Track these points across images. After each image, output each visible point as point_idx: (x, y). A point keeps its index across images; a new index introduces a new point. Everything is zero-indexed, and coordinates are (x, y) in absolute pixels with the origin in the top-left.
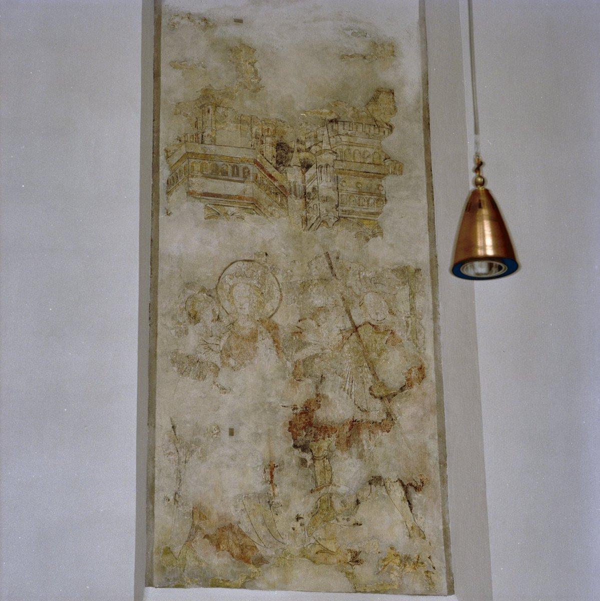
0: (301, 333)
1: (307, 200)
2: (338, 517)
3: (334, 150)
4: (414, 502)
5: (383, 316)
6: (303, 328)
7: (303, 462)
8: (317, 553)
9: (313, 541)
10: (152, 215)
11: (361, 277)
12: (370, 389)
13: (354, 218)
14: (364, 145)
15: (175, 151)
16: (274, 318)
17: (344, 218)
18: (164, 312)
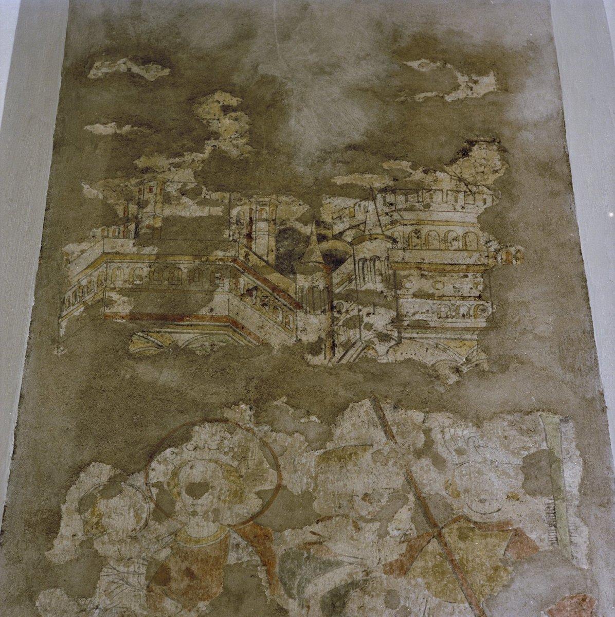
0: (320, 543)
1: (336, 314)
5: (496, 506)
6: (326, 534)
10: (27, 356)
11: (447, 436)
13: (428, 339)
15: (82, 252)
16: (263, 519)
17: (410, 339)
18: (35, 519)
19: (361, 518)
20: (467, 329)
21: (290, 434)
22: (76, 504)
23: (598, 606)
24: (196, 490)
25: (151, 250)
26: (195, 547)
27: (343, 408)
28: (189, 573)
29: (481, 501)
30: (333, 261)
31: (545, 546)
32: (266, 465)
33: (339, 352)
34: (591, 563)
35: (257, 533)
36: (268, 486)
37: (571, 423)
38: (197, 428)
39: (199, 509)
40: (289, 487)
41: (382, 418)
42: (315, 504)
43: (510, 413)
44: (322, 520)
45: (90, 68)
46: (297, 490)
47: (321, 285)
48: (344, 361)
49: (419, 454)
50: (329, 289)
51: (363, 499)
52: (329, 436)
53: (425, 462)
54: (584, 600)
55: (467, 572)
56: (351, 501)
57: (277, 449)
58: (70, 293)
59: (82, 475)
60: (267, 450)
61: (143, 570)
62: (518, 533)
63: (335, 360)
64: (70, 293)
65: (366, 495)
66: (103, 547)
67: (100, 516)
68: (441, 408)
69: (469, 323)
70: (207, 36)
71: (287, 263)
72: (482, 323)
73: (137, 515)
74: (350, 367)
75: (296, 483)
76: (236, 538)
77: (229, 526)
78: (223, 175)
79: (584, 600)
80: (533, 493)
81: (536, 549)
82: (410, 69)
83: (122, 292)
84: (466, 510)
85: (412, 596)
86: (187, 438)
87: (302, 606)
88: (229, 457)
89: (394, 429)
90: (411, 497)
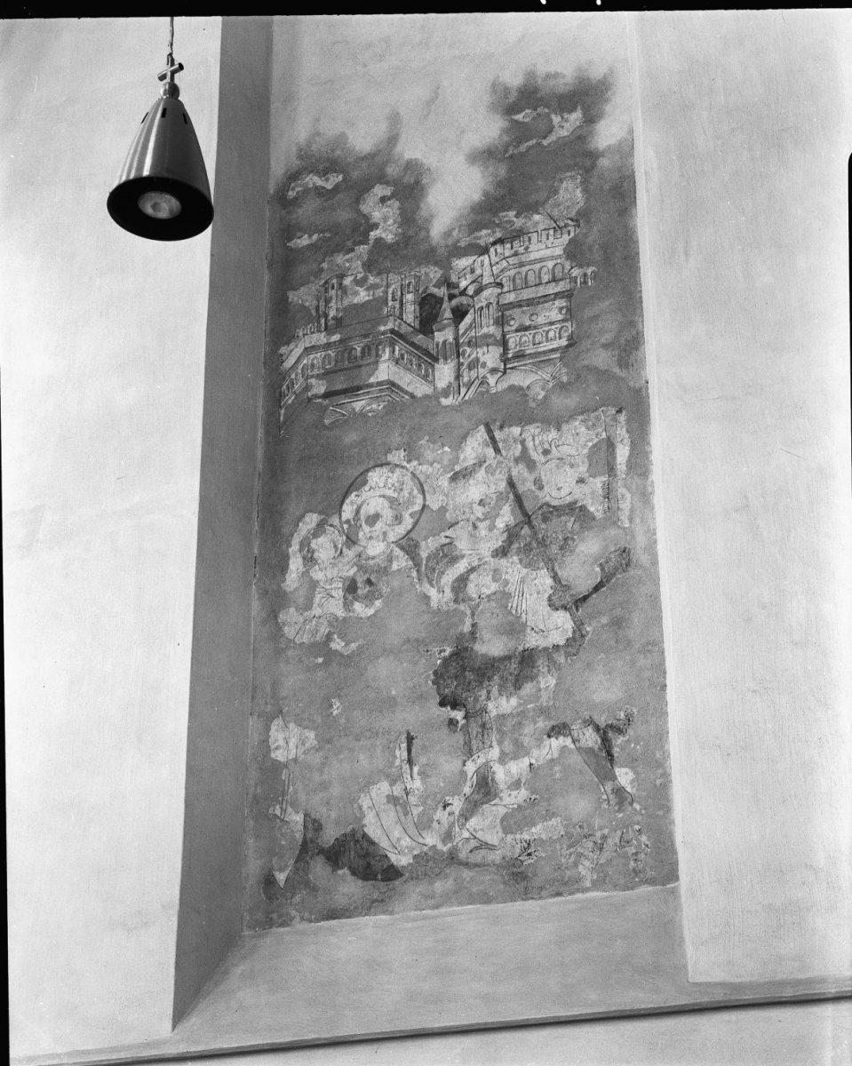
2: (501, 795)
3: (498, 280)
4: (616, 751)
7: (452, 723)
8: (471, 851)
9: (466, 835)
11: (537, 442)
12: (550, 599)
14: (541, 260)
15: (291, 351)
19: (478, 519)
20: (553, 350)
21: (431, 464)
22: (298, 547)
23: (633, 554)
24: (373, 519)
25: (336, 337)
26: (371, 562)
27: (464, 438)
28: (369, 582)
29: (558, 489)
30: (459, 314)
31: (599, 515)
32: (416, 492)
33: (463, 390)
34: (631, 522)
35: (409, 546)
36: (417, 508)
37: (624, 412)
38: (370, 474)
39: (374, 535)
40: (431, 505)
41: (493, 439)
42: (447, 515)
43: (582, 413)
44: (451, 526)
45: (288, 190)
46: (435, 507)
47: (451, 339)
48: (467, 398)
49: (517, 460)
50: (456, 339)
51: (479, 504)
52: (456, 460)
53: (521, 466)
54: (624, 551)
55: (546, 546)
56: (471, 508)
57: (422, 479)
58: (285, 387)
59: (300, 524)
60: (416, 481)
61: (340, 585)
62: (583, 508)
63: (460, 399)
64: (285, 387)
65: (481, 501)
66: (317, 575)
67: (313, 552)
68: (531, 421)
69: (555, 345)
70: (363, 139)
71: (427, 322)
72: (564, 342)
73: (335, 547)
74: (469, 402)
75: (434, 503)
76: (397, 552)
77: (393, 542)
78: (382, 258)
79: (624, 551)
80: (594, 477)
81: (594, 519)
82: (517, 121)
83: (318, 377)
84: (548, 499)
85: (510, 570)
86: (365, 482)
87: (439, 591)
88: (392, 491)
89: (500, 445)
90: (511, 496)
